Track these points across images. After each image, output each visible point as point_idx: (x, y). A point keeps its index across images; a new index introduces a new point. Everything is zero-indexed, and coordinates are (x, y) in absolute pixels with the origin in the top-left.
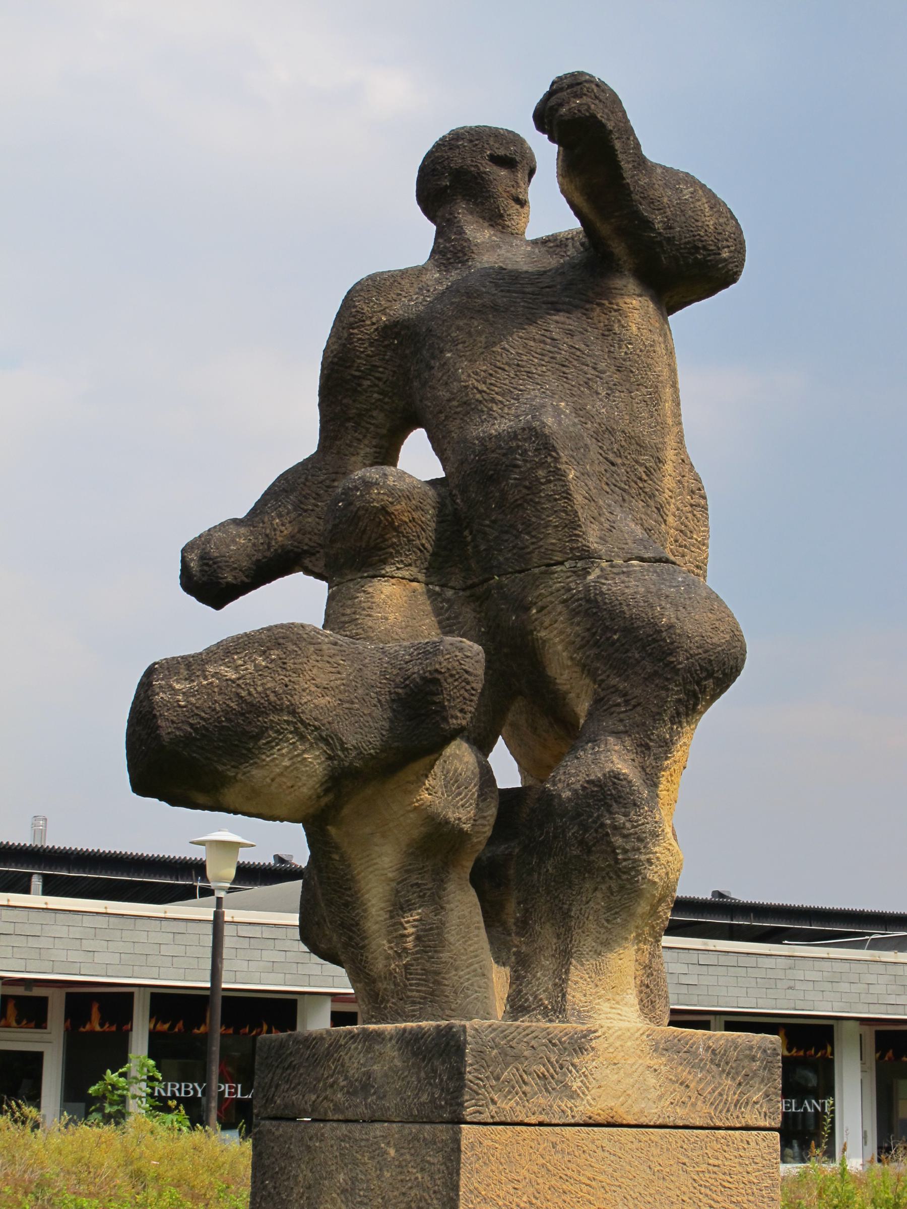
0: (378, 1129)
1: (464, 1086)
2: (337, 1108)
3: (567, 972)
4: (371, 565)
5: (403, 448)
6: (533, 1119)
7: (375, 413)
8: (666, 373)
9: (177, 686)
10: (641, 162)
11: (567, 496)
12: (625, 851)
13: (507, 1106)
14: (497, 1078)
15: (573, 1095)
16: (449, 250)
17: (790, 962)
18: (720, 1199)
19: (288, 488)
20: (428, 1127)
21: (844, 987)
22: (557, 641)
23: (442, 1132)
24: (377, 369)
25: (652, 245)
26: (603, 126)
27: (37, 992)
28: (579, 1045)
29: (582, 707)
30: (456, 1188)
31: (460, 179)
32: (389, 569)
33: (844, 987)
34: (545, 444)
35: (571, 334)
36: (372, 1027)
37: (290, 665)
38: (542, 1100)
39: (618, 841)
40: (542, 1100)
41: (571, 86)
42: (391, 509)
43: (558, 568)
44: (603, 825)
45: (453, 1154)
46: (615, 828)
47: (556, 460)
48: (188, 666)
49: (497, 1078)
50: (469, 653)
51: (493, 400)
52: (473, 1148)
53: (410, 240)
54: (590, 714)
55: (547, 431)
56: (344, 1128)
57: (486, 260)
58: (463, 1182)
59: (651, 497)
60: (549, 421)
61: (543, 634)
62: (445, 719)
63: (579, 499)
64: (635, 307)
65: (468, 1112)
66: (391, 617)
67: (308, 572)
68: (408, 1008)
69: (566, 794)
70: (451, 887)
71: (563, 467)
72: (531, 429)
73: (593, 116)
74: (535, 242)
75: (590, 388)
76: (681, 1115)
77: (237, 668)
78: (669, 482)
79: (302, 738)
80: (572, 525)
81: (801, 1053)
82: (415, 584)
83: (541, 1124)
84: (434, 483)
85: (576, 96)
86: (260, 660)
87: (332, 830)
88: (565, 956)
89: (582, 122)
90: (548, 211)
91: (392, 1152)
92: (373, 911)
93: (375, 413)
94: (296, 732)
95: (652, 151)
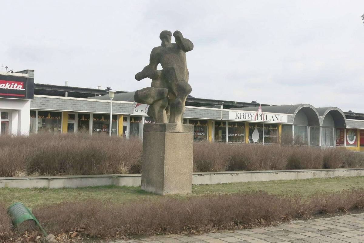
13: (170, 131)
15: (175, 130)
16: (163, 44)
17: (200, 110)
19: (146, 68)
21: (210, 114)
23: (164, 133)
24: (156, 56)
25: (184, 45)
28: (176, 125)
29: (177, 94)
30: (165, 138)
31: (165, 36)
32: (158, 80)
33: (210, 114)
34: (173, 69)
50: (166, 90)
53: (158, 43)
54: (177, 95)
57: (167, 47)
64: (182, 52)
65: (166, 131)
76: (185, 132)
80: (176, 77)
81: (202, 125)
84: (161, 70)
88: (174, 117)
89: (177, 35)
90: (173, 40)
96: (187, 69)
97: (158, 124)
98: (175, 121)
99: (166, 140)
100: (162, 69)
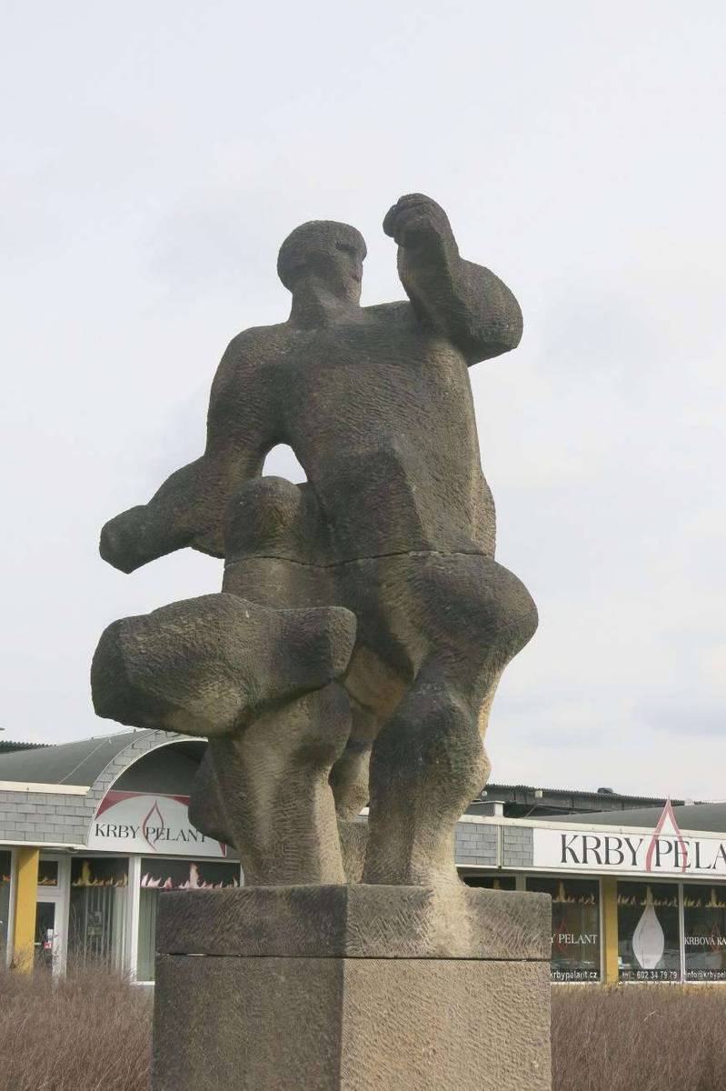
0: (270, 962)
1: (346, 931)
2: (233, 947)
3: (411, 848)
4: (263, 548)
5: (267, 457)
6: (391, 955)
7: (252, 432)
8: (470, 412)
9: (139, 639)
10: (459, 260)
11: (411, 503)
12: (456, 762)
13: (375, 945)
14: (367, 925)
15: (417, 937)
16: (305, 311)
18: (511, 1010)
19: (180, 486)
20: (314, 960)
22: (402, 609)
23: (328, 964)
25: (458, 314)
26: (439, 236)
27: (513, 875)
28: (422, 900)
29: (417, 657)
30: (340, 1004)
31: (316, 257)
32: (276, 552)
34: (391, 465)
35: (404, 382)
36: (263, 888)
37: (221, 624)
38: (396, 941)
39: (453, 755)
40: (396, 941)
41: (414, 205)
42: (281, 508)
43: (404, 556)
44: (442, 743)
45: (337, 981)
46: (451, 746)
47: (404, 477)
48: (146, 624)
49: (367, 925)
50: (345, 619)
51: (350, 430)
52: (351, 976)
54: (426, 663)
55: (396, 456)
56: (239, 962)
58: (345, 1000)
59: (463, 504)
60: (397, 448)
61: (390, 603)
62: (331, 666)
63: (419, 505)
65: (349, 950)
66: (279, 588)
67: (196, 547)
68: (285, 873)
69: (416, 722)
70: (318, 785)
71: (409, 483)
72: (384, 453)
73: (433, 229)
74: (368, 309)
75: (420, 424)
76: (488, 950)
77: (182, 626)
78: (473, 494)
79: (229, 678)
80: (414, 525)
82: (294, 564)
83: (396, 958)
84: (300, 486)
85: (419, 213)
86: (200, 621)
87: (236, 744)
88: (409, 837)
89: (418, 227)
91: (283, 979)
92: (262, 802)
93: (252, 432)
94: (225, 673)
95: (466, 253)
96: (482, 478)
97: (279, 888)
98: (416, 866)
99: (345, 1027)
100: (304, 479)
